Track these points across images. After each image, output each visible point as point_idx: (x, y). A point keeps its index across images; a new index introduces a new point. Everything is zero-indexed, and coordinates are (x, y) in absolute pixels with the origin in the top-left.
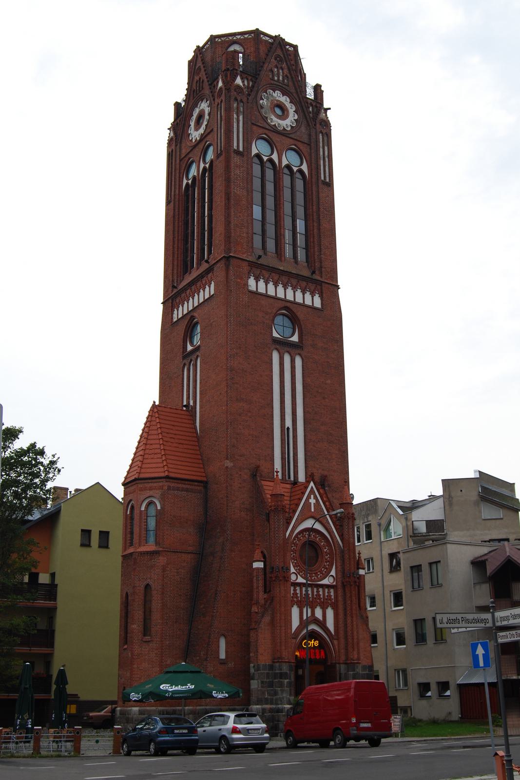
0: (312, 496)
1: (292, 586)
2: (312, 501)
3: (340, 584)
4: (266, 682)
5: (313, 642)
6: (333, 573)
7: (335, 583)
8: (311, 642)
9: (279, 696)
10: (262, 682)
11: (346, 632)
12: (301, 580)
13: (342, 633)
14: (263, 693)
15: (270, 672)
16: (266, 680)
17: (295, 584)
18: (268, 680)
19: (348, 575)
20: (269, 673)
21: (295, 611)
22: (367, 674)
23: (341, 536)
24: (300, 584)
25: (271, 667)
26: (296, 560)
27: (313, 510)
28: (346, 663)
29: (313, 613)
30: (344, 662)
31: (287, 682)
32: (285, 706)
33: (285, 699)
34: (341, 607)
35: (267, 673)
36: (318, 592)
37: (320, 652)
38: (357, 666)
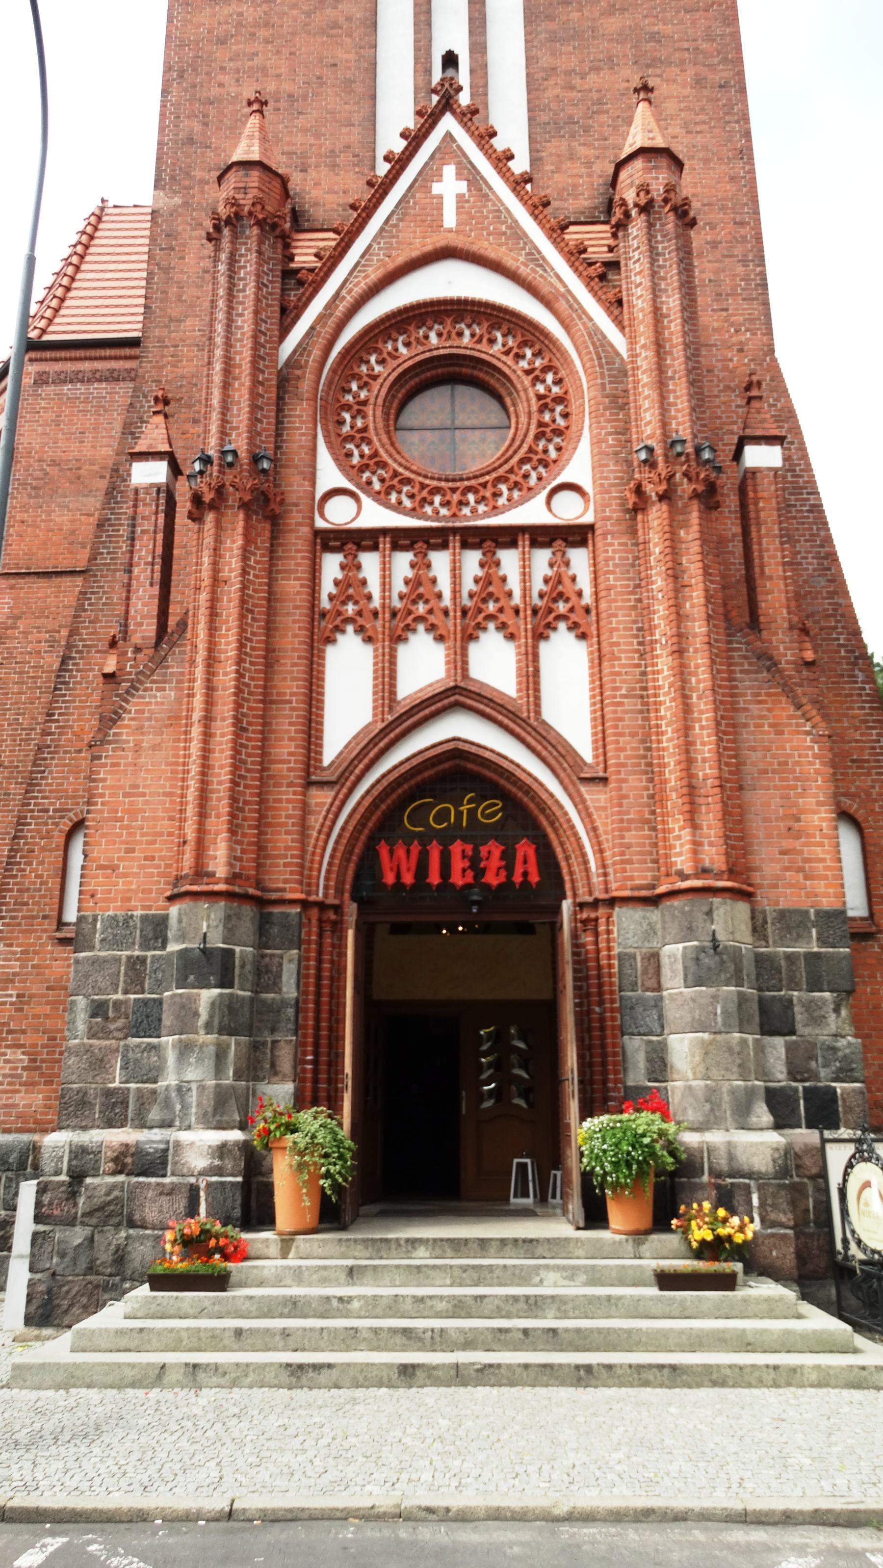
0: (449, 171)
1: (327, 548)
2: (449, 186)
3: (614, 512)
4: (117, 1004)
5: (464, 808)
6: (579, 467)
7: (588, 518)
8: (458, 803)
9: (169, 1080)
10: (98, 1010)
11: (648, 737)
12: (375, 516)
13: (626, 748)
14: (99, 1064)
15: (150, 954)
16: (119, 996)
17: (354, 541)
18: (132, 996)
19: (643, 456)
20: (142, 960)
21: (349, 664)
22: (812, 958)
23: (616, 305)
24: (367, 539)
25: (156, 930)
26: (369, 442)
27: (450, 219)
28: (654, 901)
29: (459, 662)
30: (644, 893)
31: (213, 1004)
32: (184, 1136)
33: (193, 1098)
34: (618, 623)
35: (129, 958)
36: (490, 563)
37: (508, 857)
38: (709, 913)
